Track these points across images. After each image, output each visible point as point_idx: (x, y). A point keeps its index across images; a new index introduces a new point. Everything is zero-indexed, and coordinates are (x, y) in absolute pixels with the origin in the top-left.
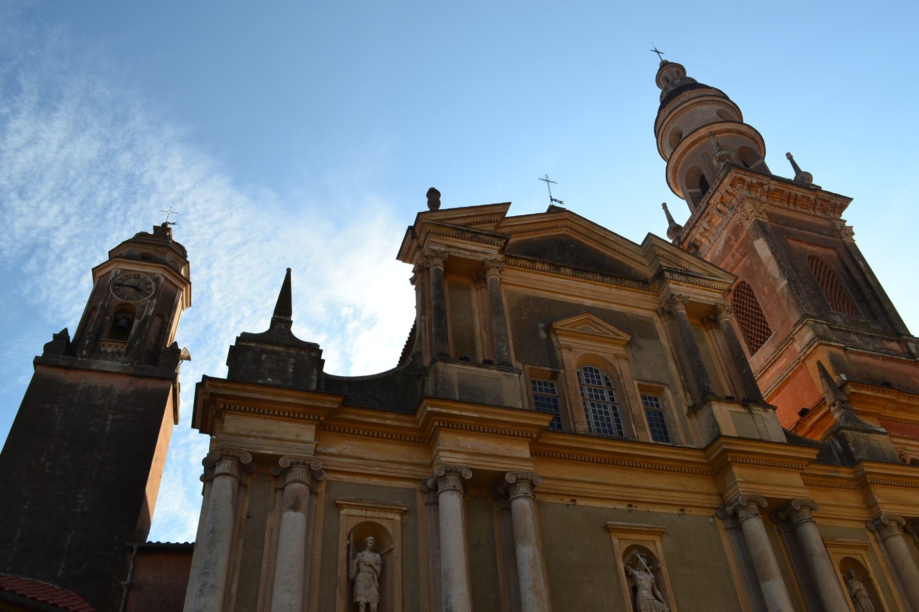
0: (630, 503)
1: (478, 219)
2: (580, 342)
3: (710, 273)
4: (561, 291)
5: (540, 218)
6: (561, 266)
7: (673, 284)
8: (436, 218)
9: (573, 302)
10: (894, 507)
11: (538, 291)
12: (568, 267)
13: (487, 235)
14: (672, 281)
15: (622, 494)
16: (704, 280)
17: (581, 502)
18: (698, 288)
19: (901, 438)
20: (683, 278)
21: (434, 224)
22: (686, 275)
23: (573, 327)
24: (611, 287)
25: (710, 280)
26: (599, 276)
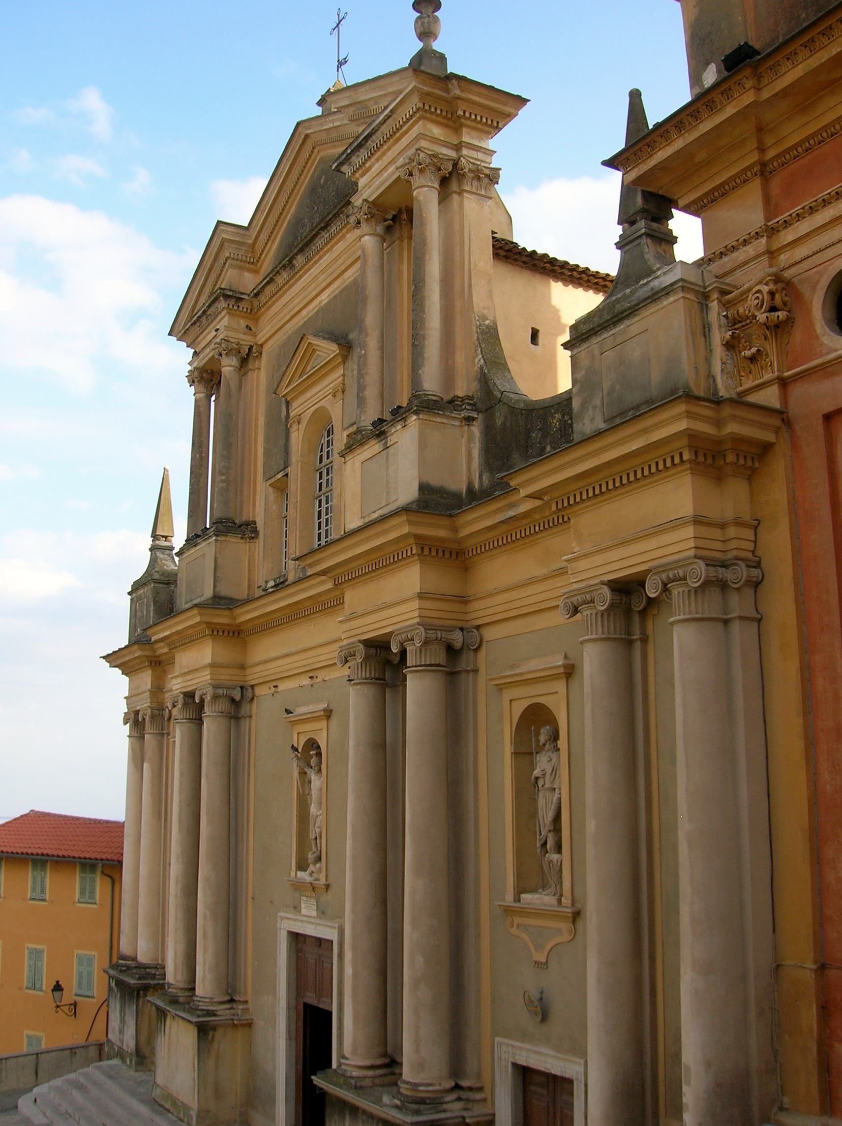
0: (311, 673)
1: (213, 277)
2: (308, 395)
3: (394, 93)
4: (301, 305)
5: (280, 176)
6: (290, 261)
7: (362, 176)
8: (183, 324)
9: (311, 314)
10: (598, 559)
11: (288, 326)
12: (296, 254)
13: (210, 306)
14: (357, 175)
15: (305, 662)
16: (385, 126)
17: (282, 686)
18: (389, 149)
19: (812, 210)
20: (363, 153)
21: (183, 334)
22: (360, 146)
23: (300, 376)
24: (344, 236)
25: (388, 117)
26: (323, 233)
